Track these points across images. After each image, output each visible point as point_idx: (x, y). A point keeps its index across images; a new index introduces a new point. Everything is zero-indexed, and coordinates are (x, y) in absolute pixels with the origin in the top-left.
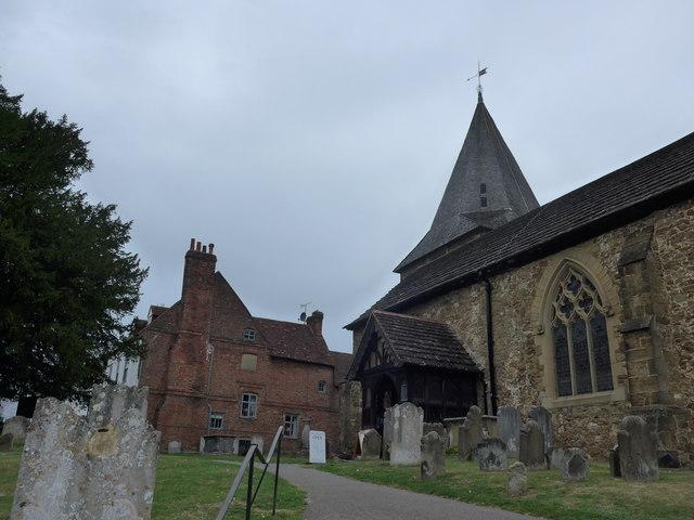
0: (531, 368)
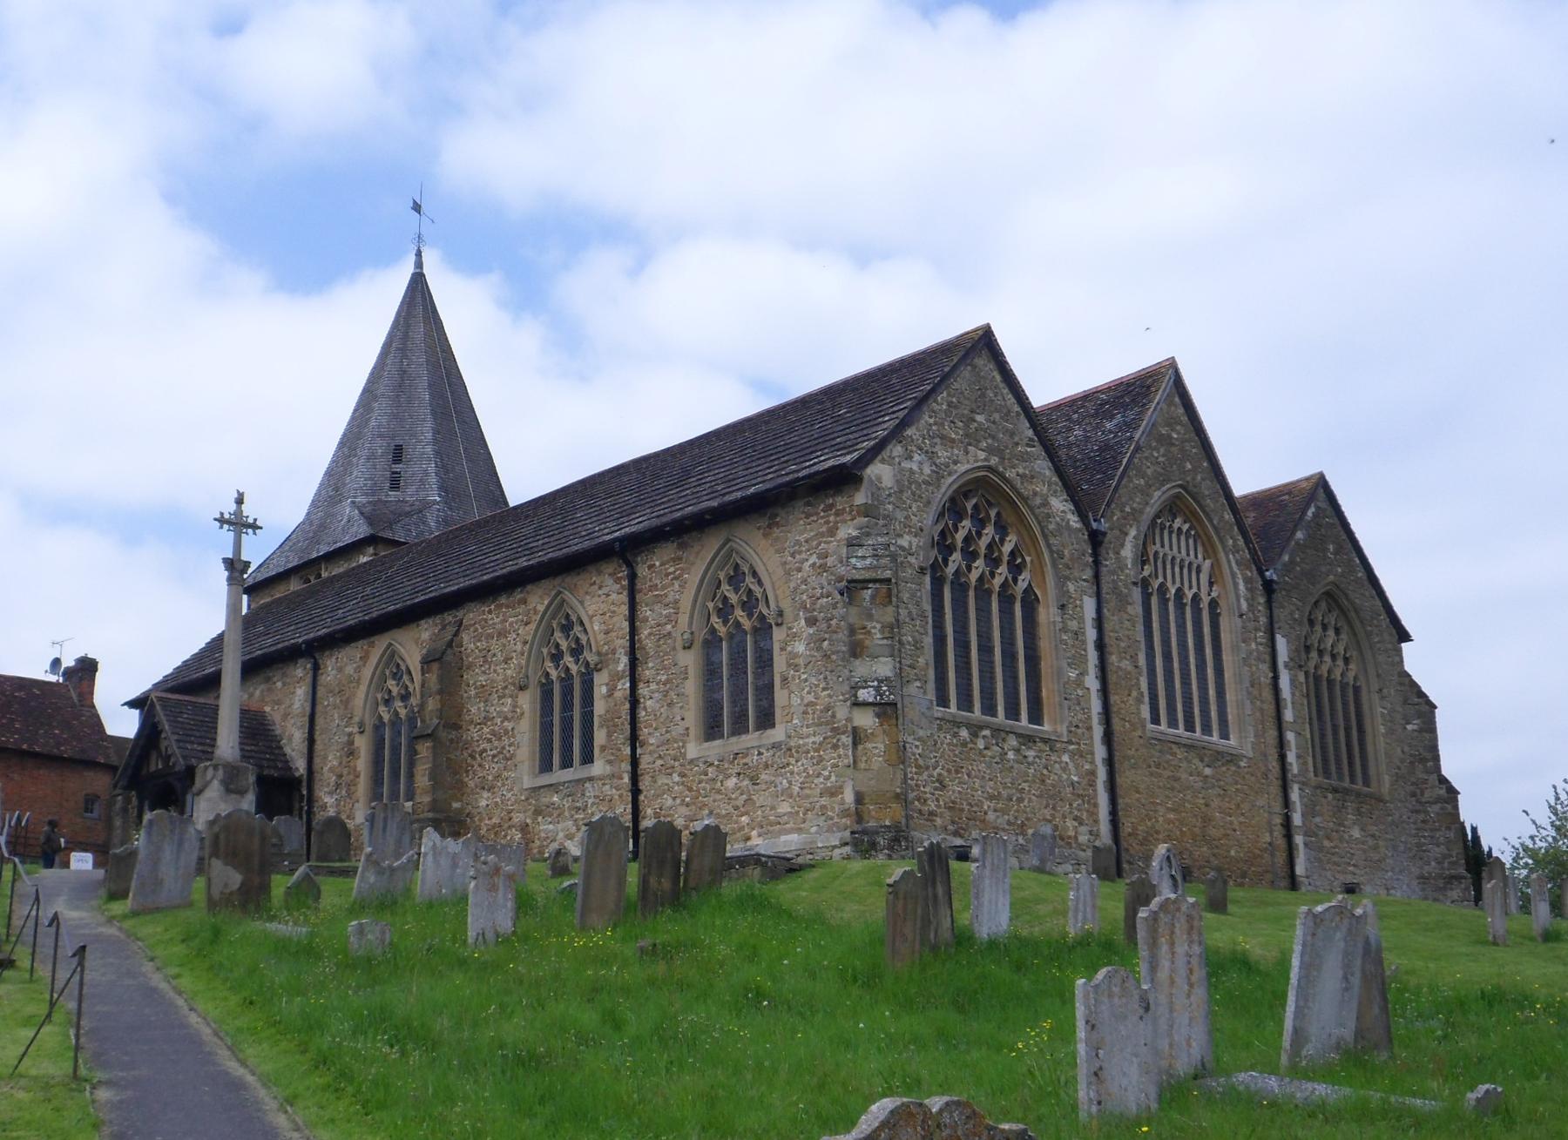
0: (349, 773)
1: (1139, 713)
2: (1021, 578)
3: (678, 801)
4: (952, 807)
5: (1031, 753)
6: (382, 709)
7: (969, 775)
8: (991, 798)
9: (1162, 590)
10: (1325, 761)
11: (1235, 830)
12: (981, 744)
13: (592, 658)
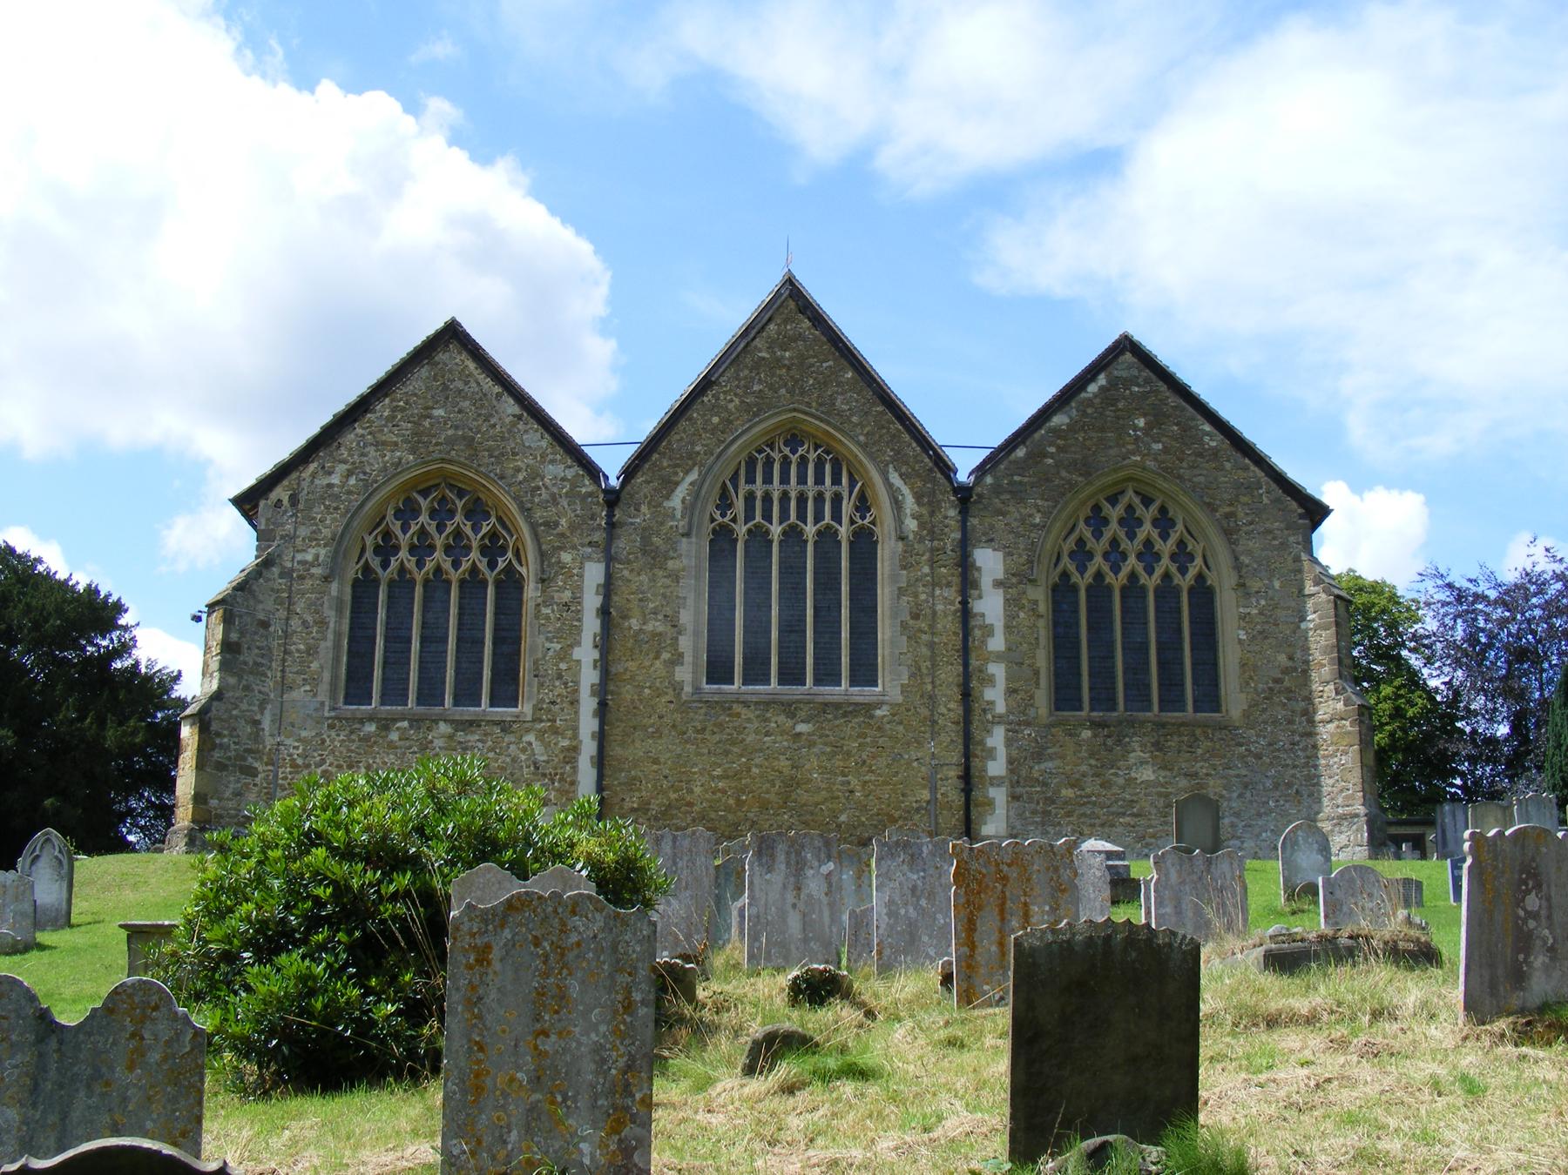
12: (394, 736)
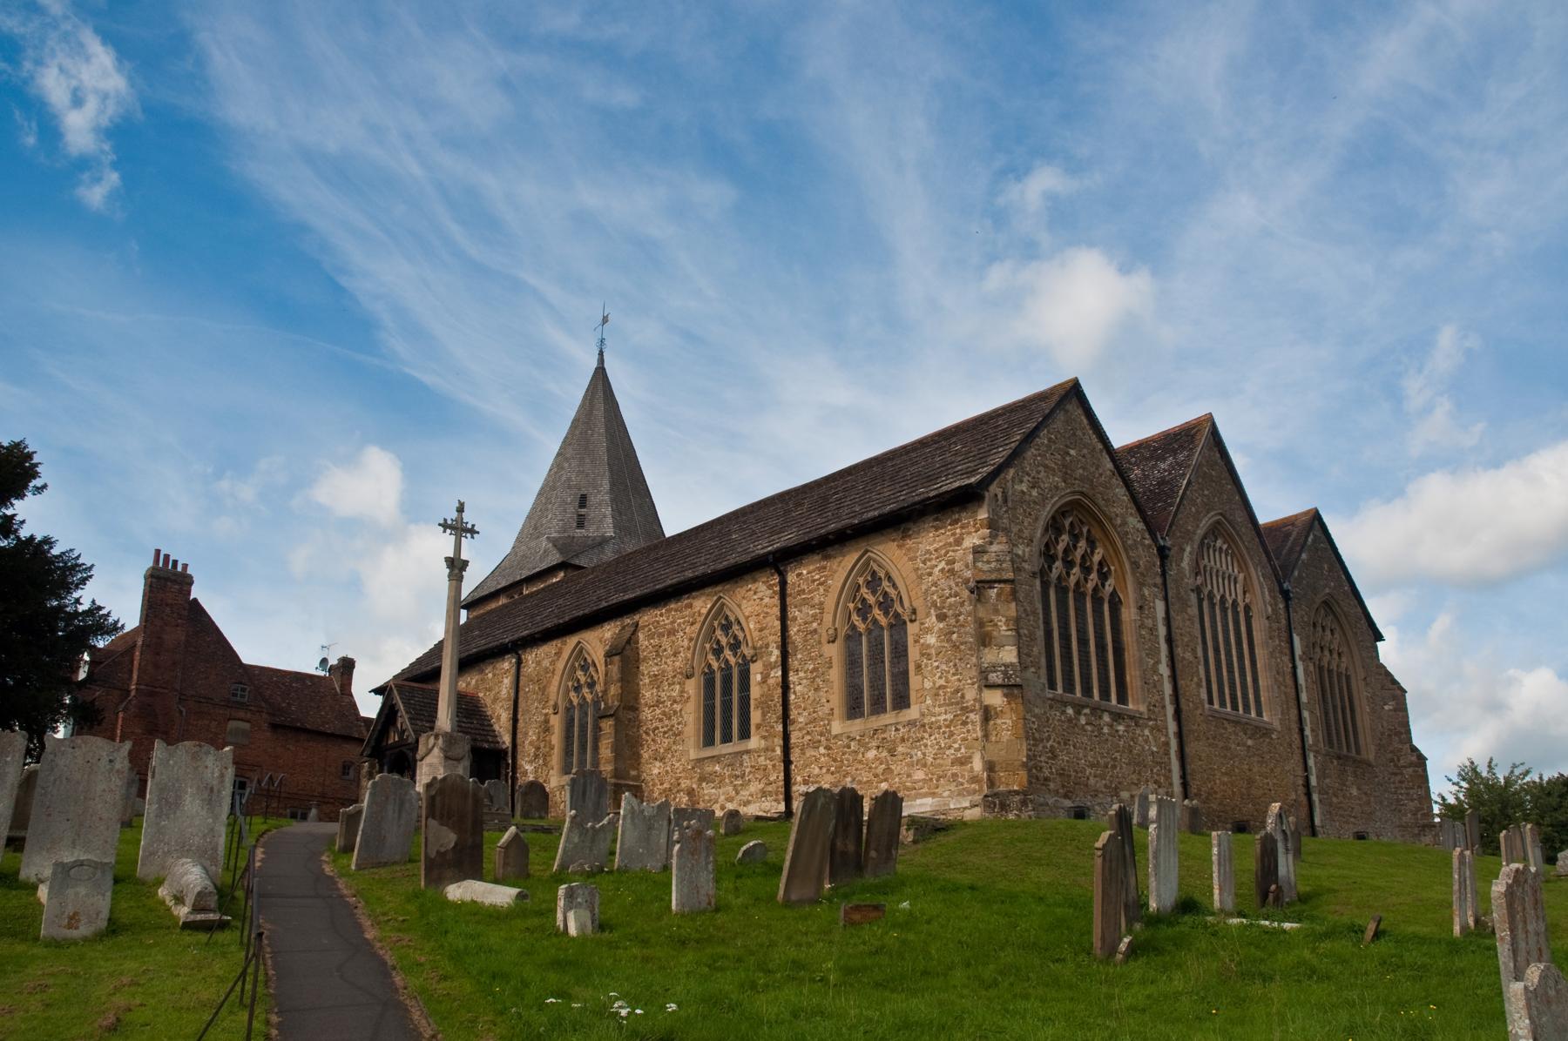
1: (1199, 695)
2: (1107, 584)
3: (824, 770)
4: (1062, 773)
5: (1121, 728)
6: (572, 694)
7: (1074, 747)
8: (1092, 766)
9: (1211, 596)
10: (1329, 734)
11: (1270, 790)
13: (748, 652)
